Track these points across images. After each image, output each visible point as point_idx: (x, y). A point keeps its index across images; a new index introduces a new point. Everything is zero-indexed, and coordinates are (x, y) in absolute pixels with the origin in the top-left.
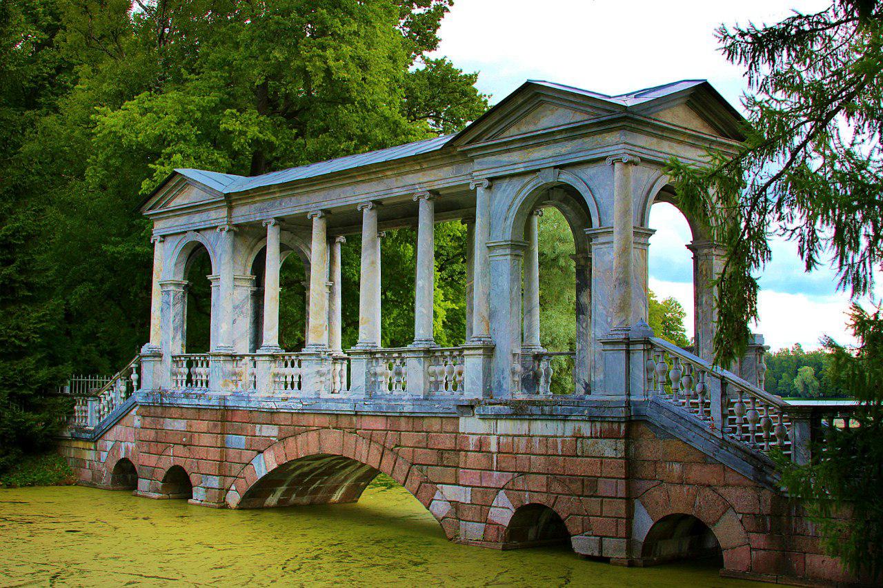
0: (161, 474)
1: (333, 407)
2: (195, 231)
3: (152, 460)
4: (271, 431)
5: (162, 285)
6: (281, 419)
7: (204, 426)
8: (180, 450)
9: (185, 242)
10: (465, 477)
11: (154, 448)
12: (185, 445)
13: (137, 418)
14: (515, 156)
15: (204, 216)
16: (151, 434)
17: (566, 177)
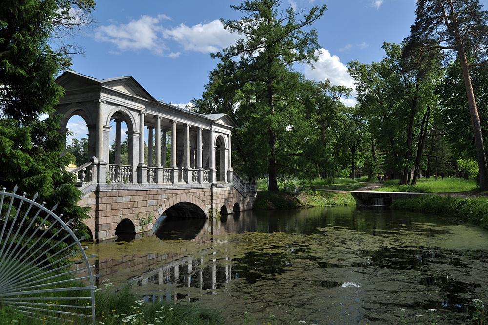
0: (115, 226)
1: (184, 187)
2: (126, 107)
3: (109, 220)
4: (164, 197)
5: (104, 127)
6: (168, 192)
7: (140, 198)
8: (126, 211)
9: (118, 109)
10: (214, 202)
11: (109, 213)
12: (129, 208)
13: (90, 199)
14: (218, 128)
15: (134, 103)
16: (109, 206)
17: (222, 135)
